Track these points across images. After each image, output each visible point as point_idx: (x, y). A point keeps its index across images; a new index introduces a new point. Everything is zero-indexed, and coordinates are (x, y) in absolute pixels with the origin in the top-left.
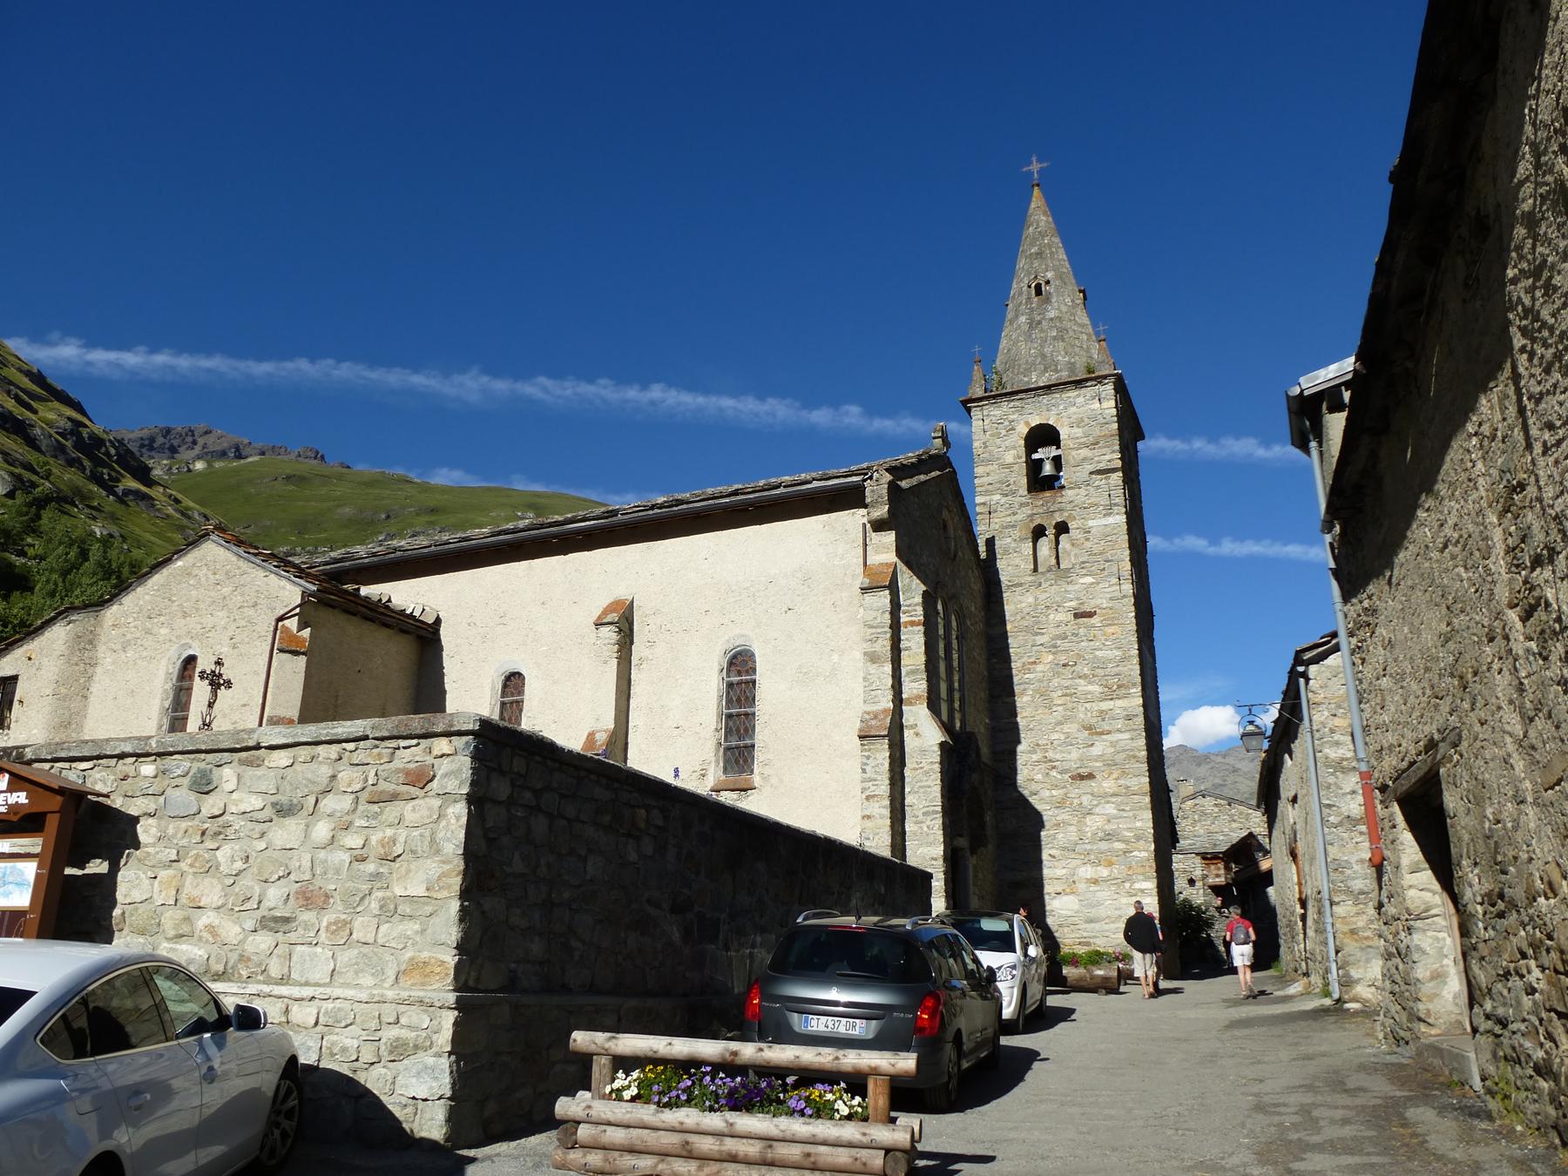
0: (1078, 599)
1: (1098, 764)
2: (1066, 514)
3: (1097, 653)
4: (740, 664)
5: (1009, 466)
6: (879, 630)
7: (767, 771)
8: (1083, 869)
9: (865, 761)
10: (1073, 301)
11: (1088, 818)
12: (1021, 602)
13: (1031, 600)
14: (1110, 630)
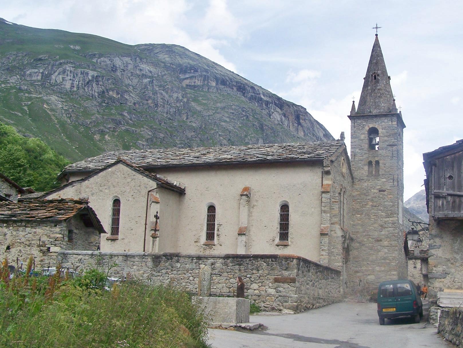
0: (381, 186)
1: (383, 237)
2: (379, 158)
3: (386, 203)
4: (285, 208)
5: (362, 140)
6: (326, 204)
7: (292, 240)
8: (377, 267)
9: (321, 240)
10: (386, 82)
11: (379, 253)
12: (363, 185)
13: (366, 185)
14: (389, 196)
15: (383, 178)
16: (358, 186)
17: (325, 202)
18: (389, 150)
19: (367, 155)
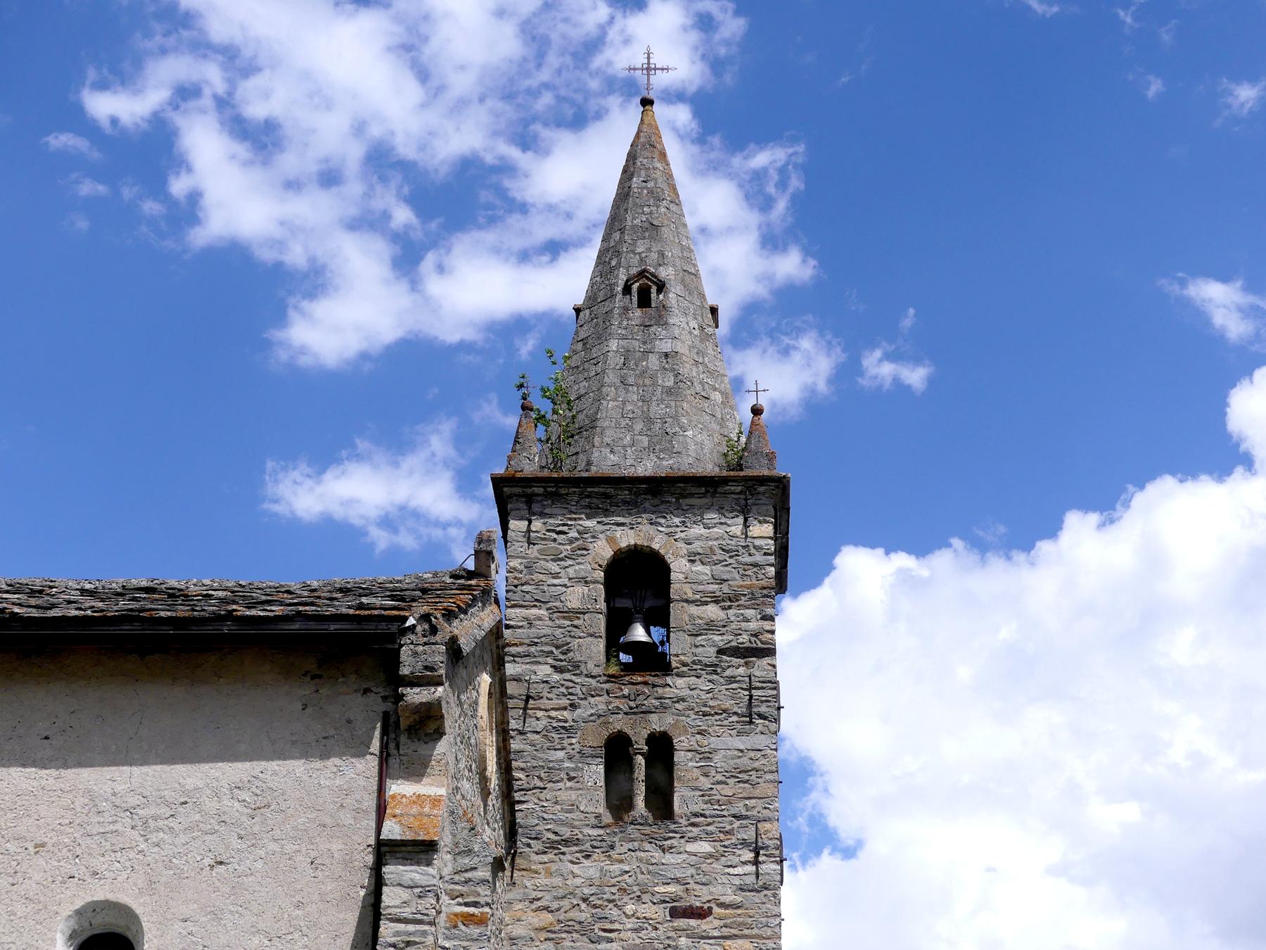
0: (677, 880)
2: (669, 719)
6: (411, 928)
10: (702, 328)
15: (694, 839)
16: (542, 880)
17: (407, 912)
18: (732, 680)
19: (600, 703)
